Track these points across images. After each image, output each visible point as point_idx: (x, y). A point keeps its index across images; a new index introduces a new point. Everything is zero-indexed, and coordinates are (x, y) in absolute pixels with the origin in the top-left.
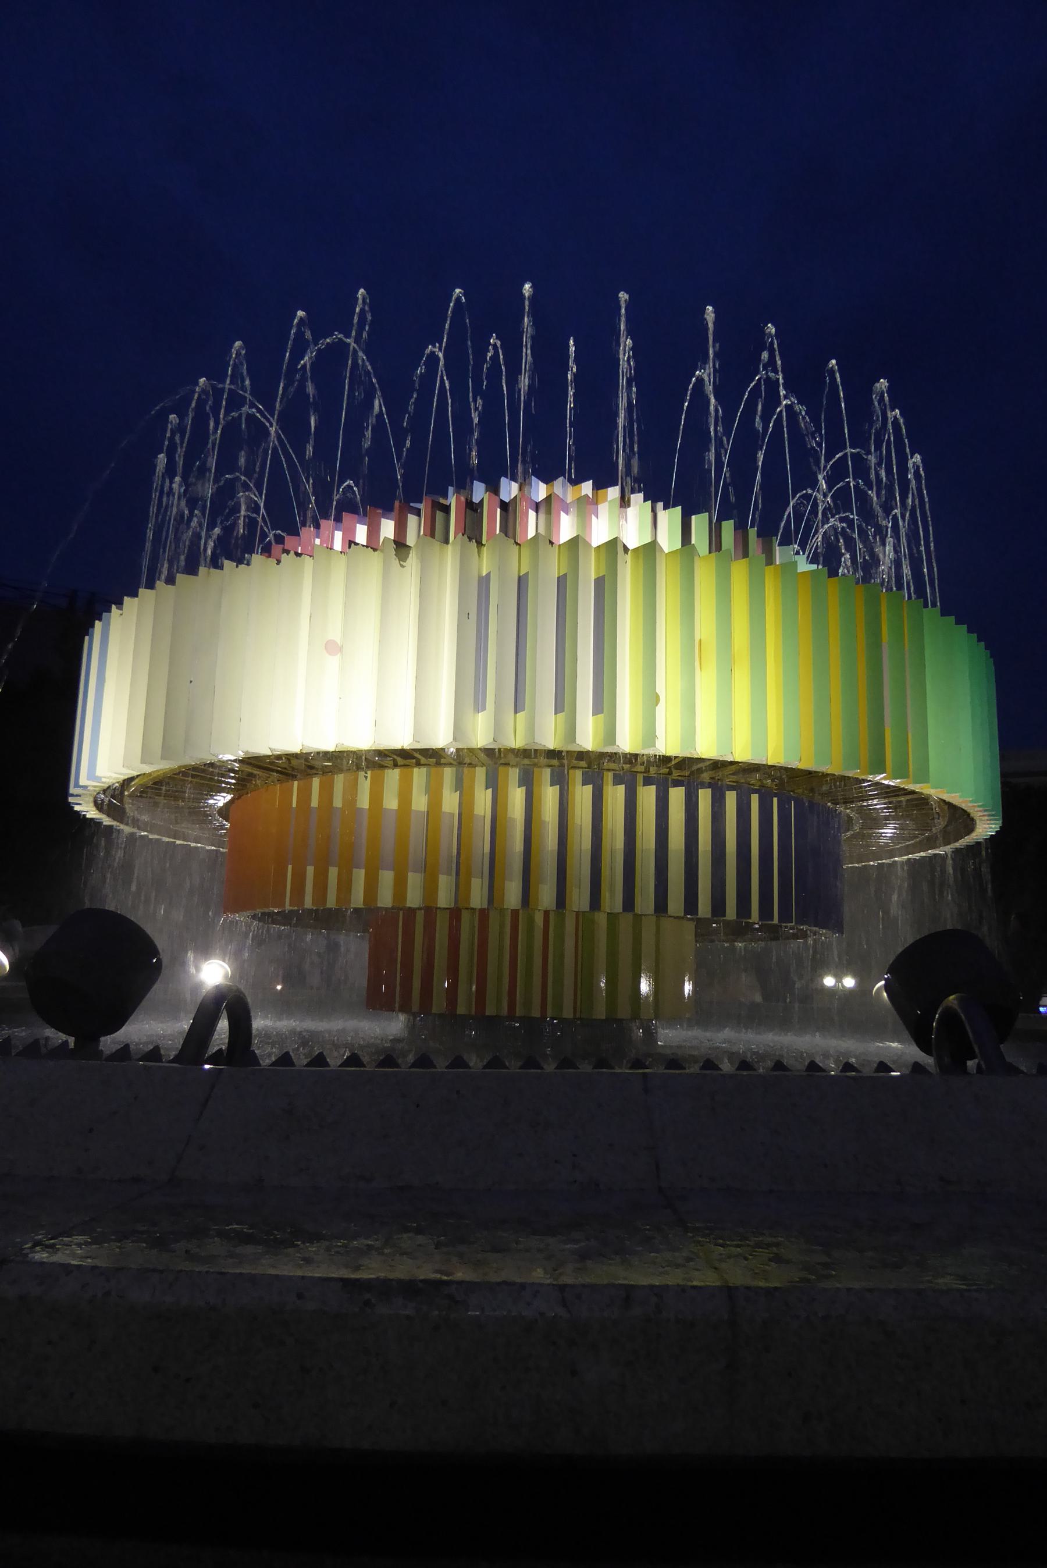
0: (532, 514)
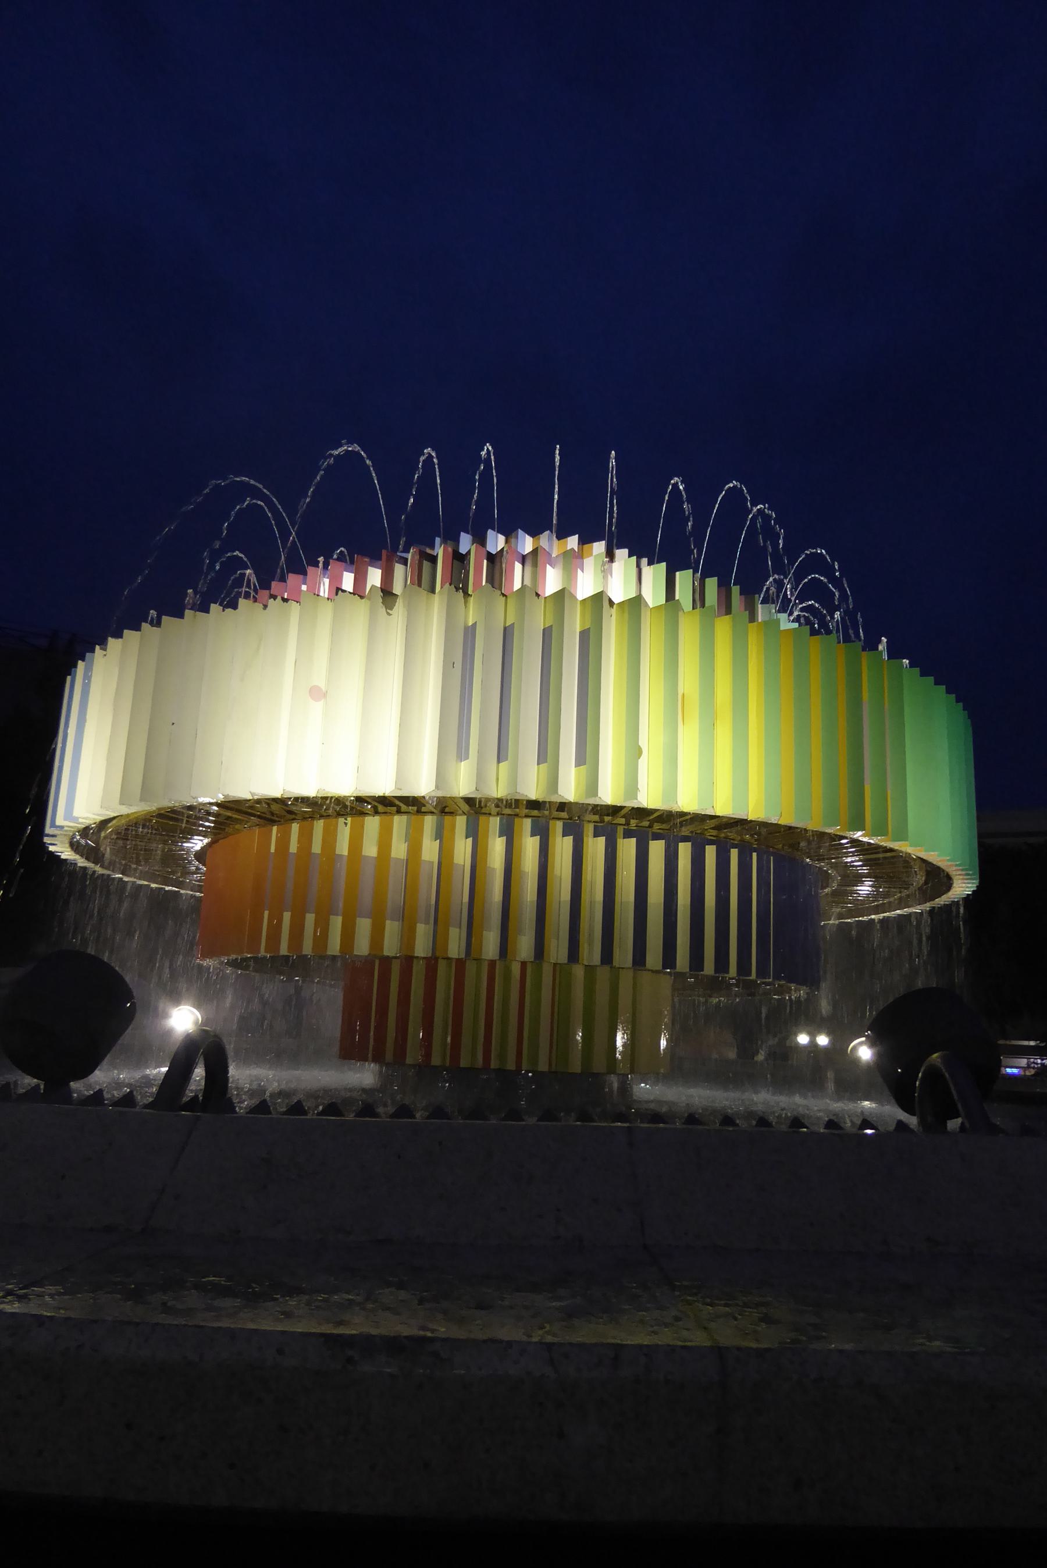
0: (518, 566)
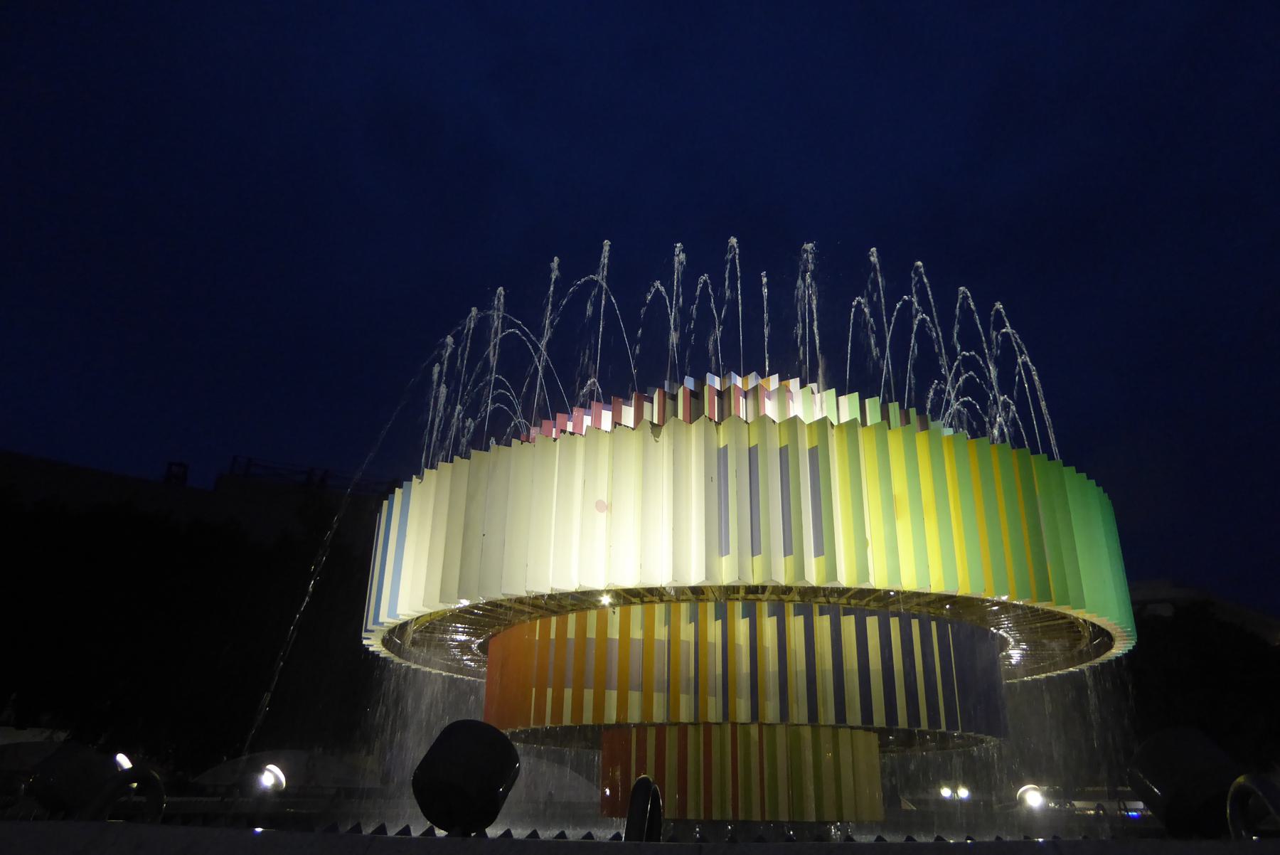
0: (742, 400)
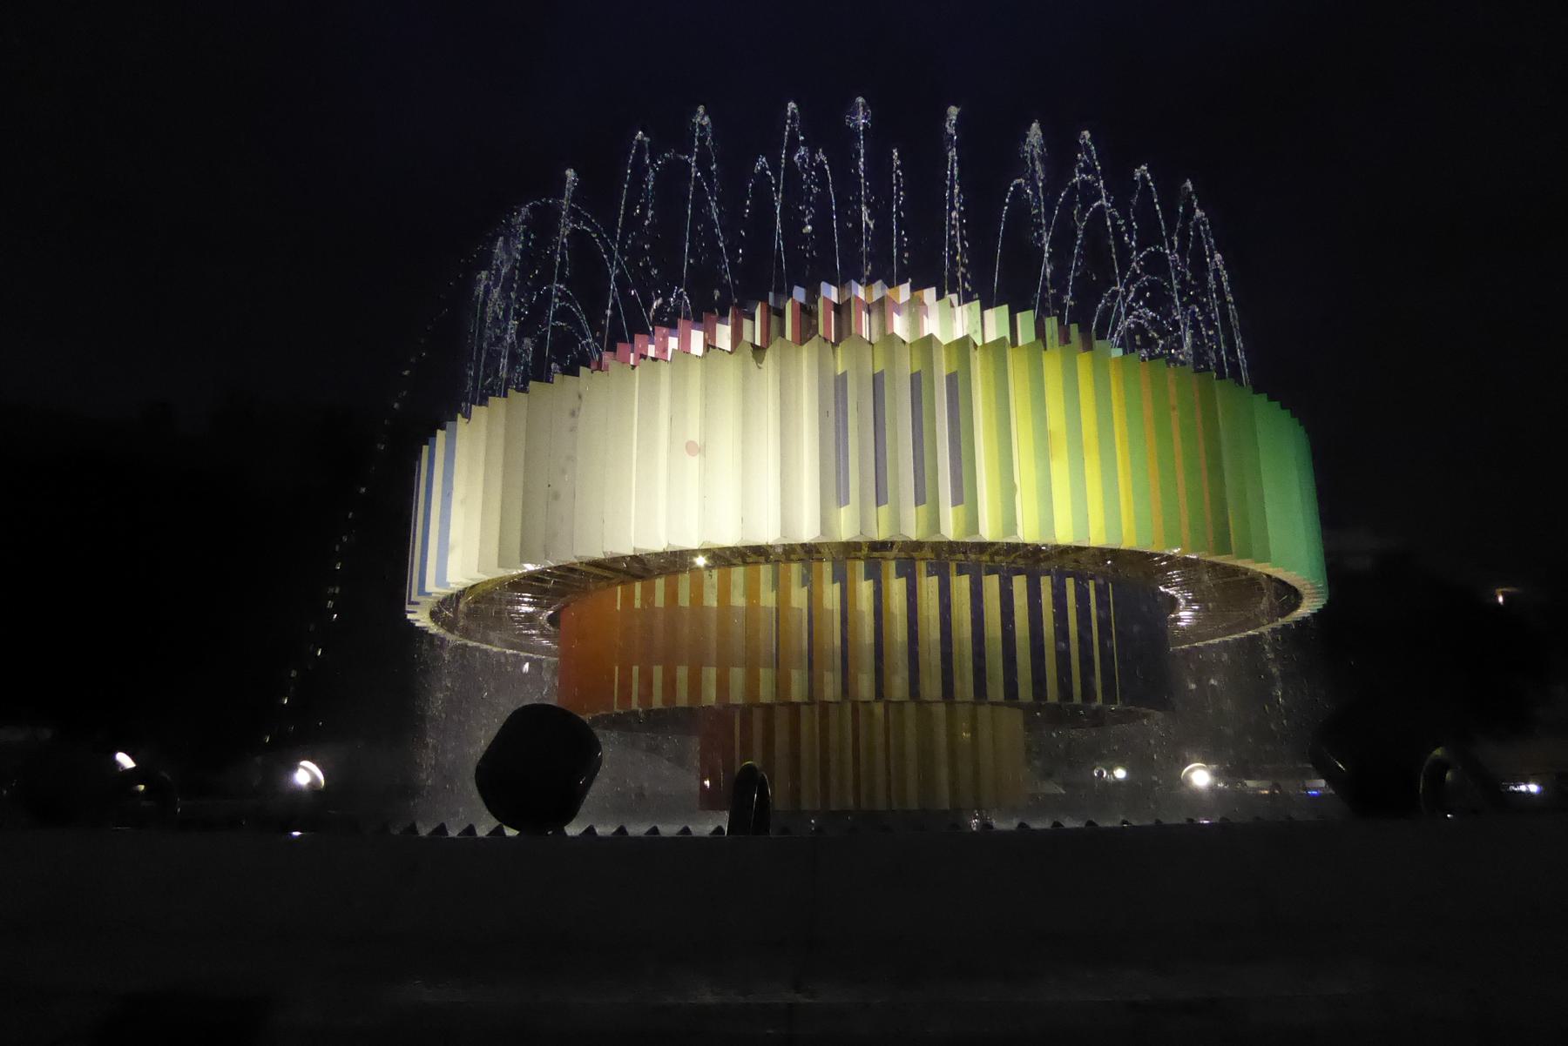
0: (865, 316)
